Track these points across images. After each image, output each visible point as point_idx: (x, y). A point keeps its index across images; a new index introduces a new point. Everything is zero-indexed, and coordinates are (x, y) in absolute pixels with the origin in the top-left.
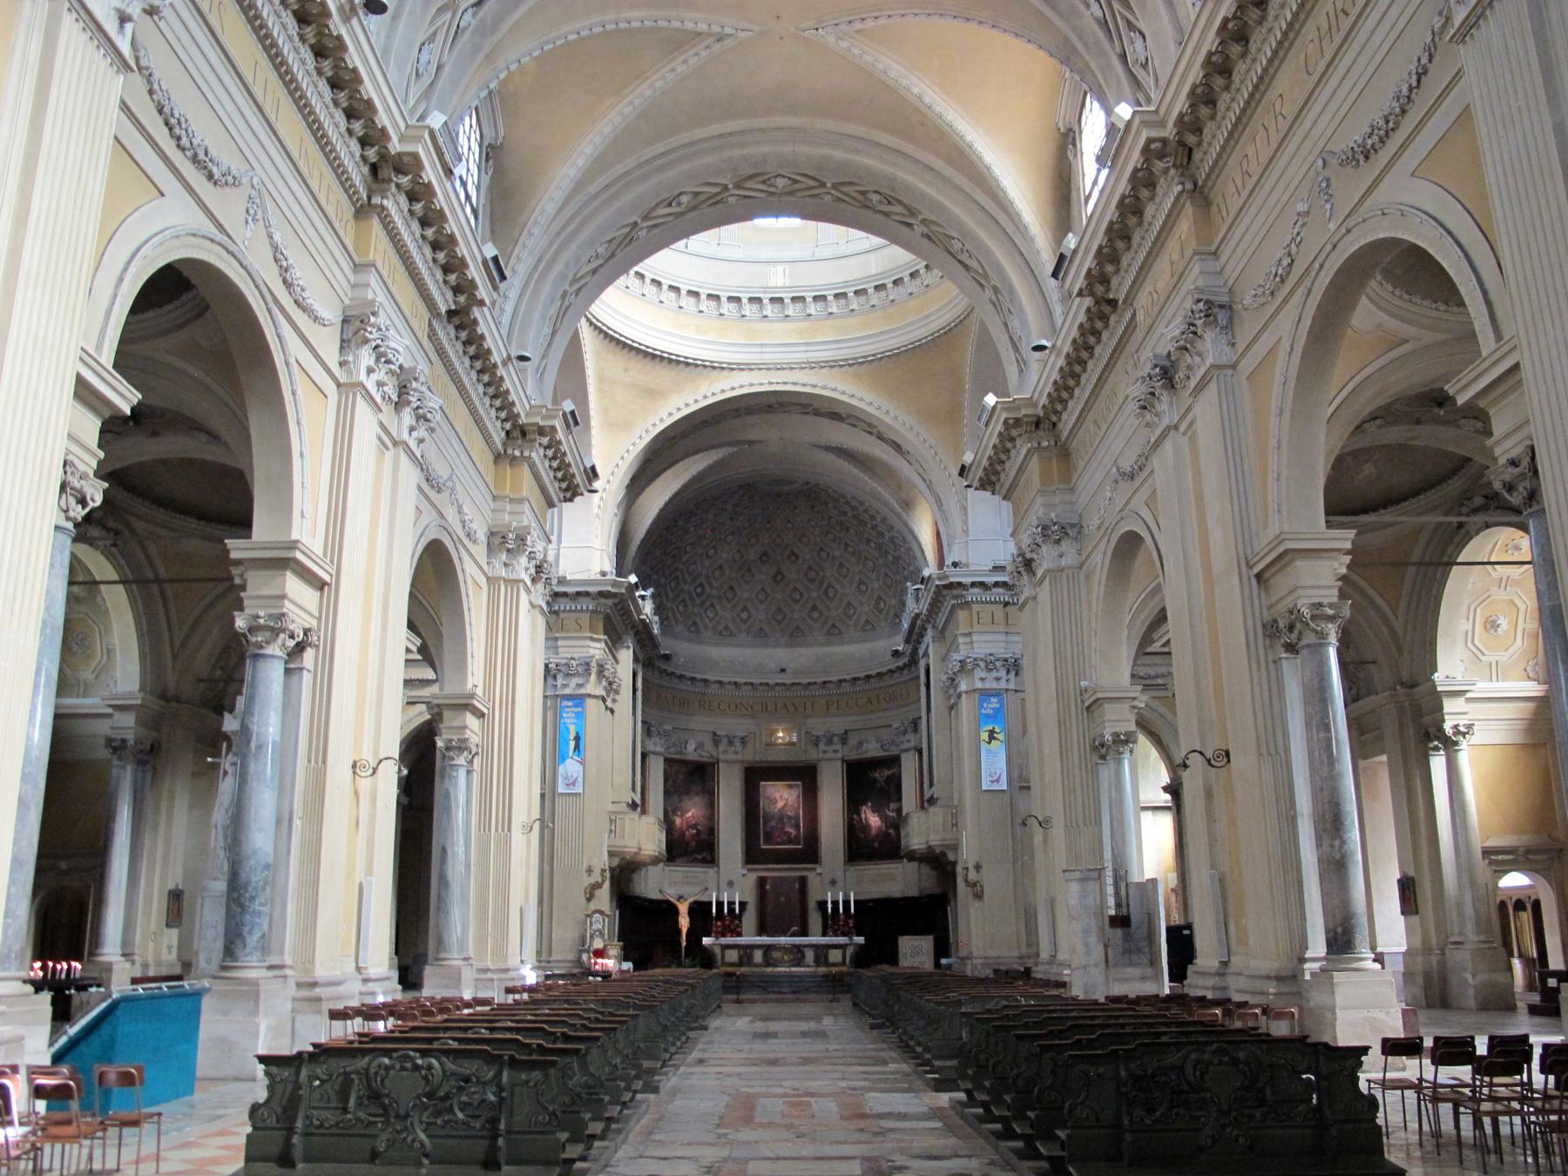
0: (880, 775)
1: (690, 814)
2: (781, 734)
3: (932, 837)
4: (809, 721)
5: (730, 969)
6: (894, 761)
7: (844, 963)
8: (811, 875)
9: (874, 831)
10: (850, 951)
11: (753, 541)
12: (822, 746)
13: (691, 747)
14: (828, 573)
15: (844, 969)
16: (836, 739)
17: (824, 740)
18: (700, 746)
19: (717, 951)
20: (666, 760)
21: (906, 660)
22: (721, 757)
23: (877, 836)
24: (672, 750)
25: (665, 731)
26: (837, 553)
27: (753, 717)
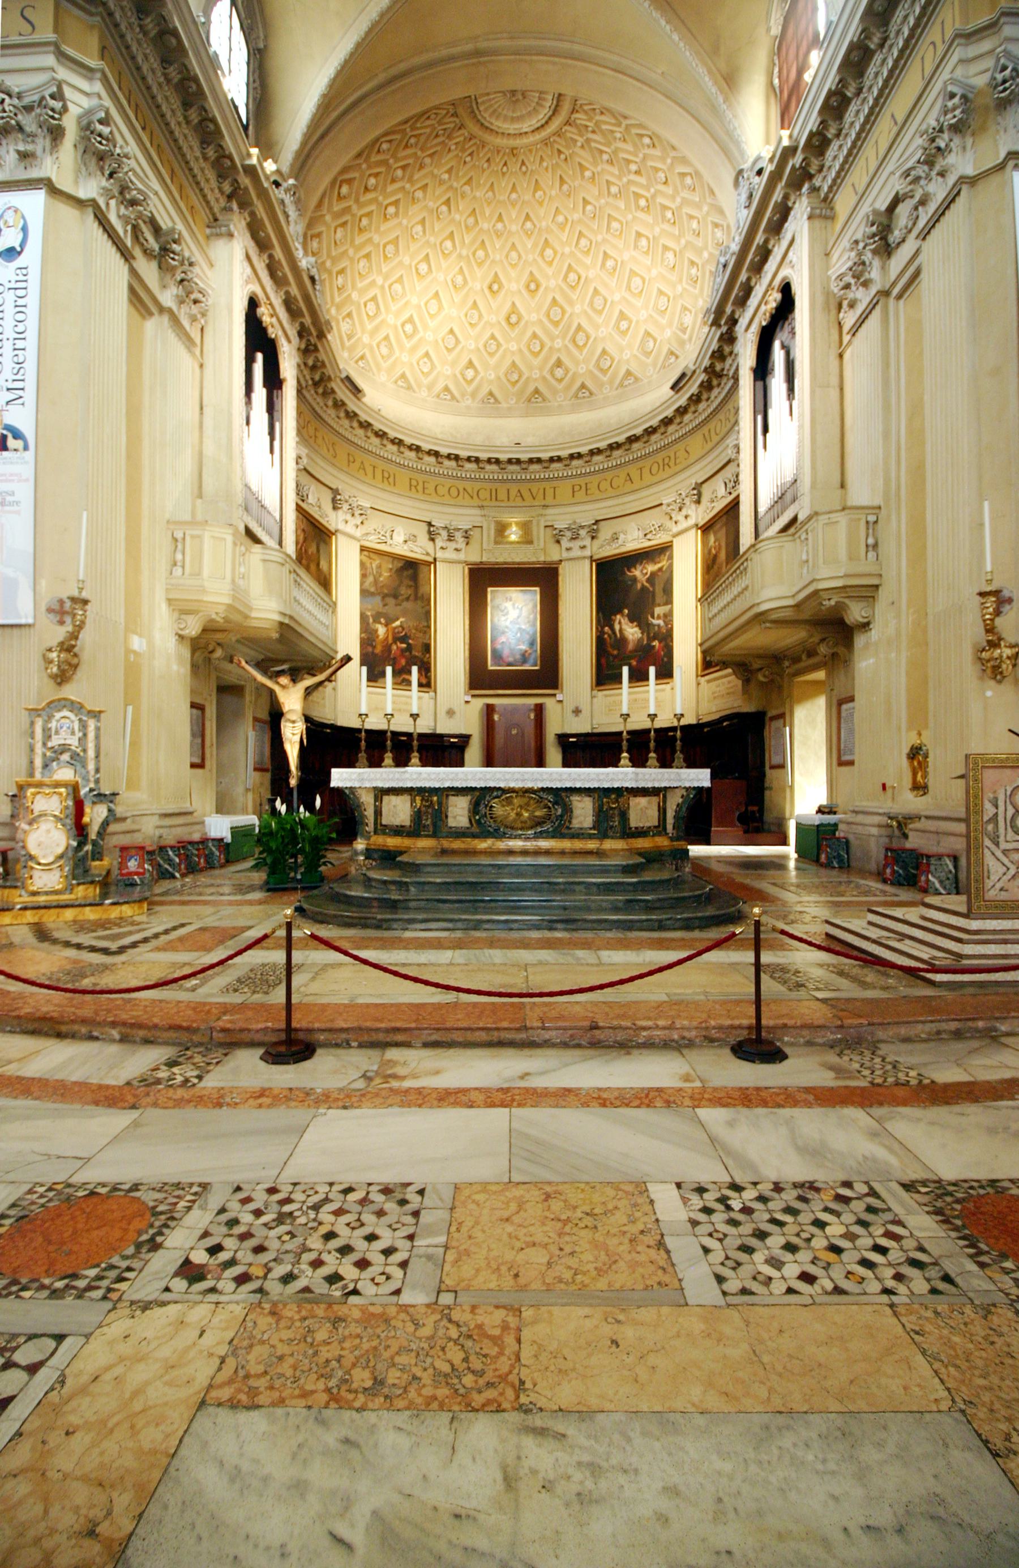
0: (640, 573)
1: (398, 623)
2: (514, 528)
3: (824, 572)
4: (550, 511)
5: (392, 842)
6: (665, 549)
7: (661, 828)
8: (549, 703)
9: (631, 646)
10: (673, 803)
11: (480, 253)
12: (565, 543)
13: (399, 537)
14: (578, 309)
15: (663, 842)
16: (583, 533)
17: (569, 534)
18: (413, 538)
19: (367, 800)
20: (363, 549)
21: (693, 388)
22: (440, 555)
23: (635, 651)
24: (372, 538)
25: (361, 508)
26: (591, 274)
27: (482, 507)
